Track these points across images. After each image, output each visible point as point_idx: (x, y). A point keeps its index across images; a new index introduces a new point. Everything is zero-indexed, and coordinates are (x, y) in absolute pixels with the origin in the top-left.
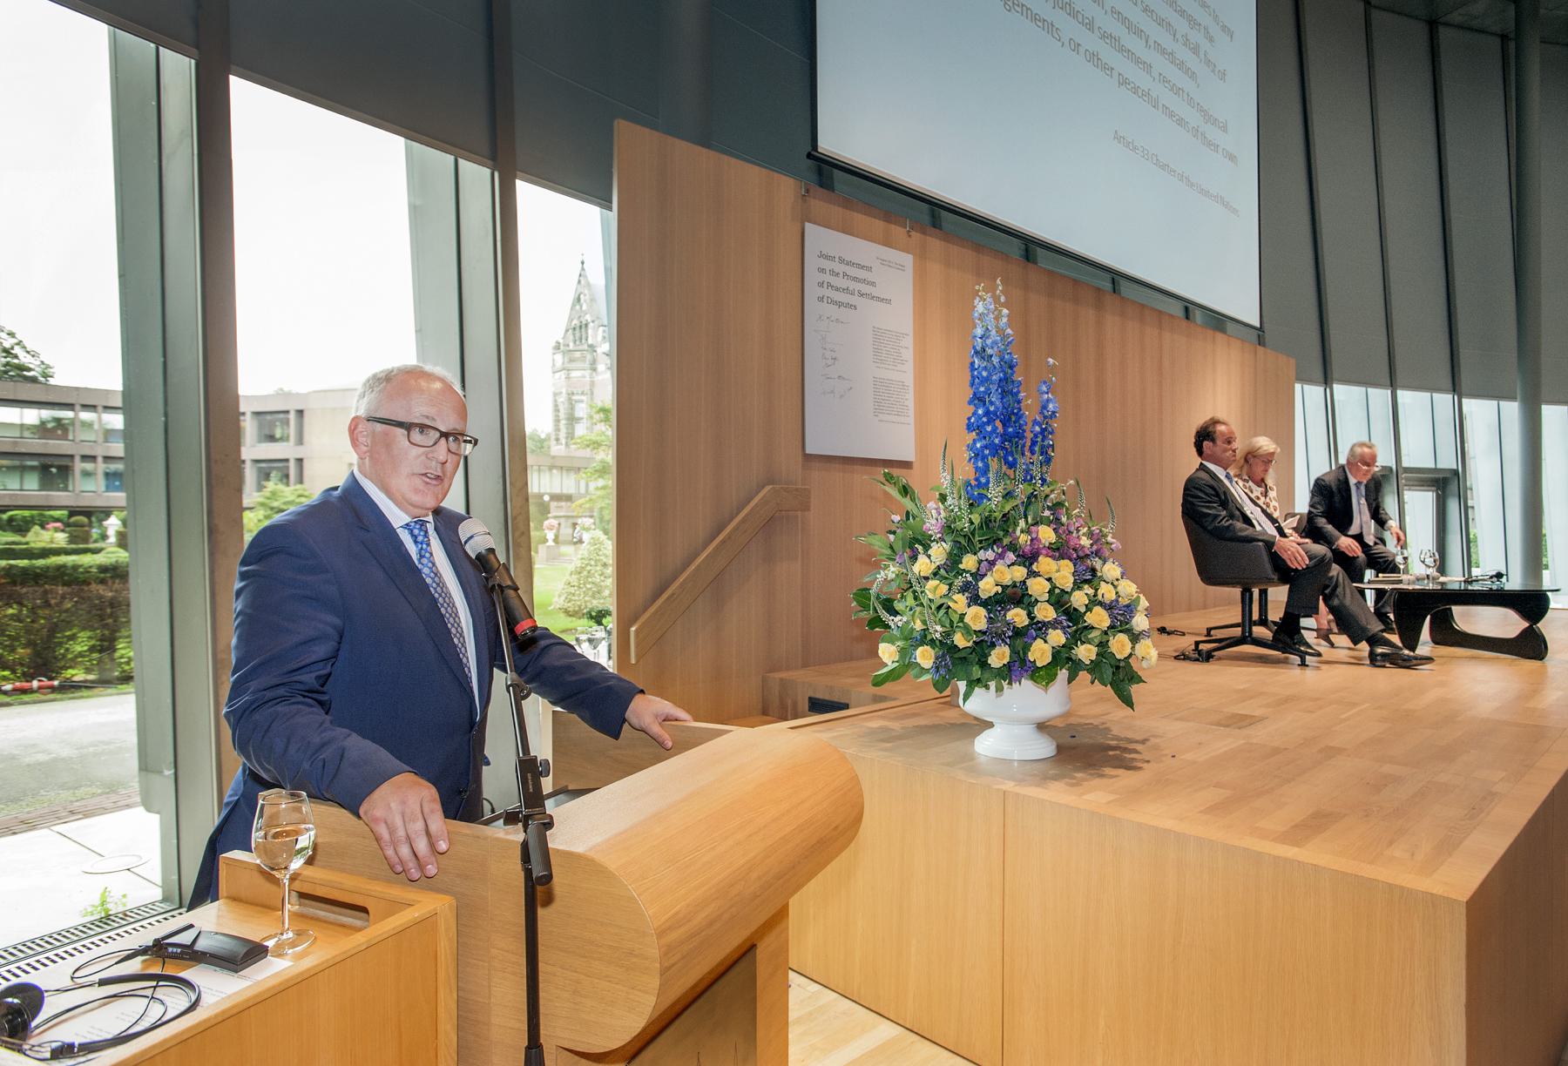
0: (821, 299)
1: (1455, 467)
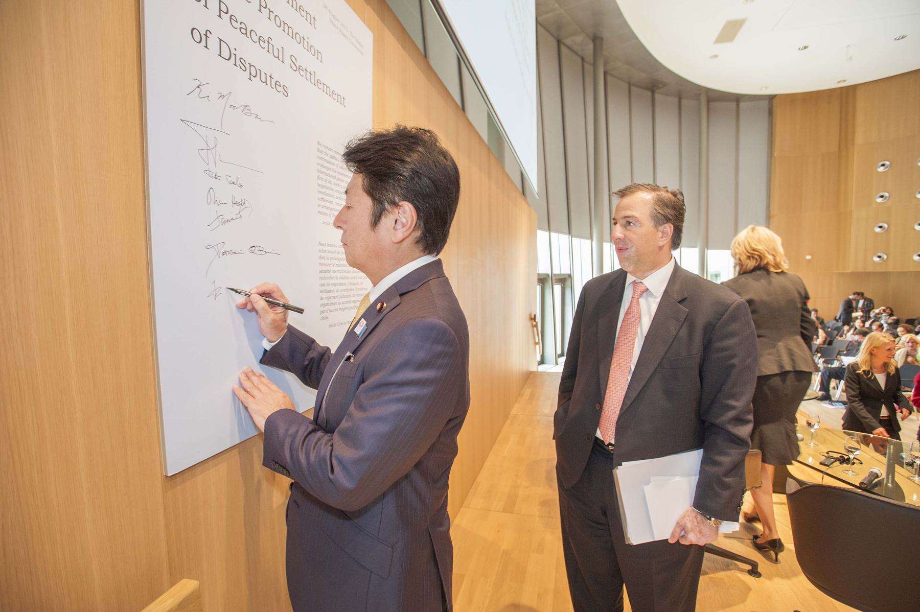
1: (569, 273)
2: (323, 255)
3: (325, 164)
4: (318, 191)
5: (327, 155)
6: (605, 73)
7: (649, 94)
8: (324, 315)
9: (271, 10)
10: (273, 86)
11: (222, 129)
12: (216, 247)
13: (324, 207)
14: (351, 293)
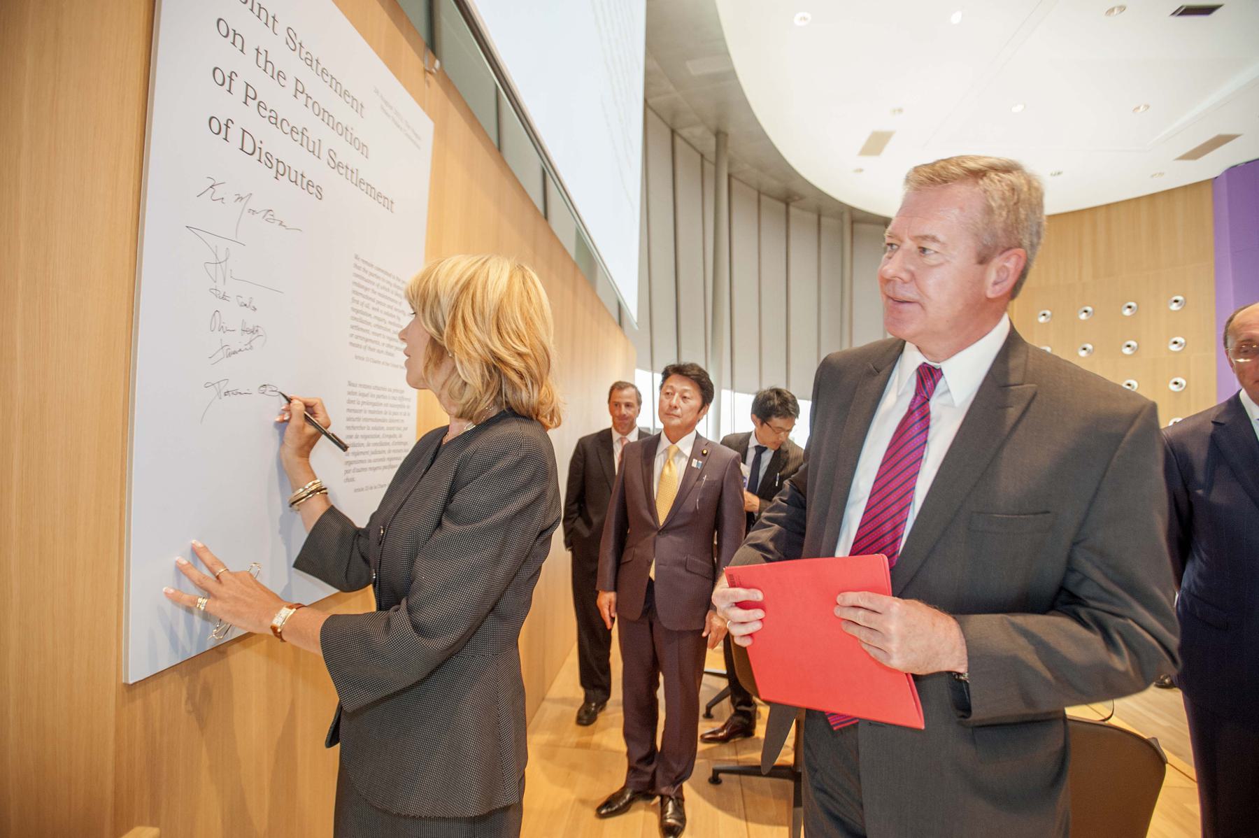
0: (222, 128)
2: (352, 398)
3: (363, 283)
4: (352, 317)
5: (366, 272)
6: (730, 176)
7: (783, 206)
8: (350, 476)
9: (309, 95)
10: (305, 186)
11: (236, 237)
12: (217, 385)
13: (357, 337)
14: (386, 448)
